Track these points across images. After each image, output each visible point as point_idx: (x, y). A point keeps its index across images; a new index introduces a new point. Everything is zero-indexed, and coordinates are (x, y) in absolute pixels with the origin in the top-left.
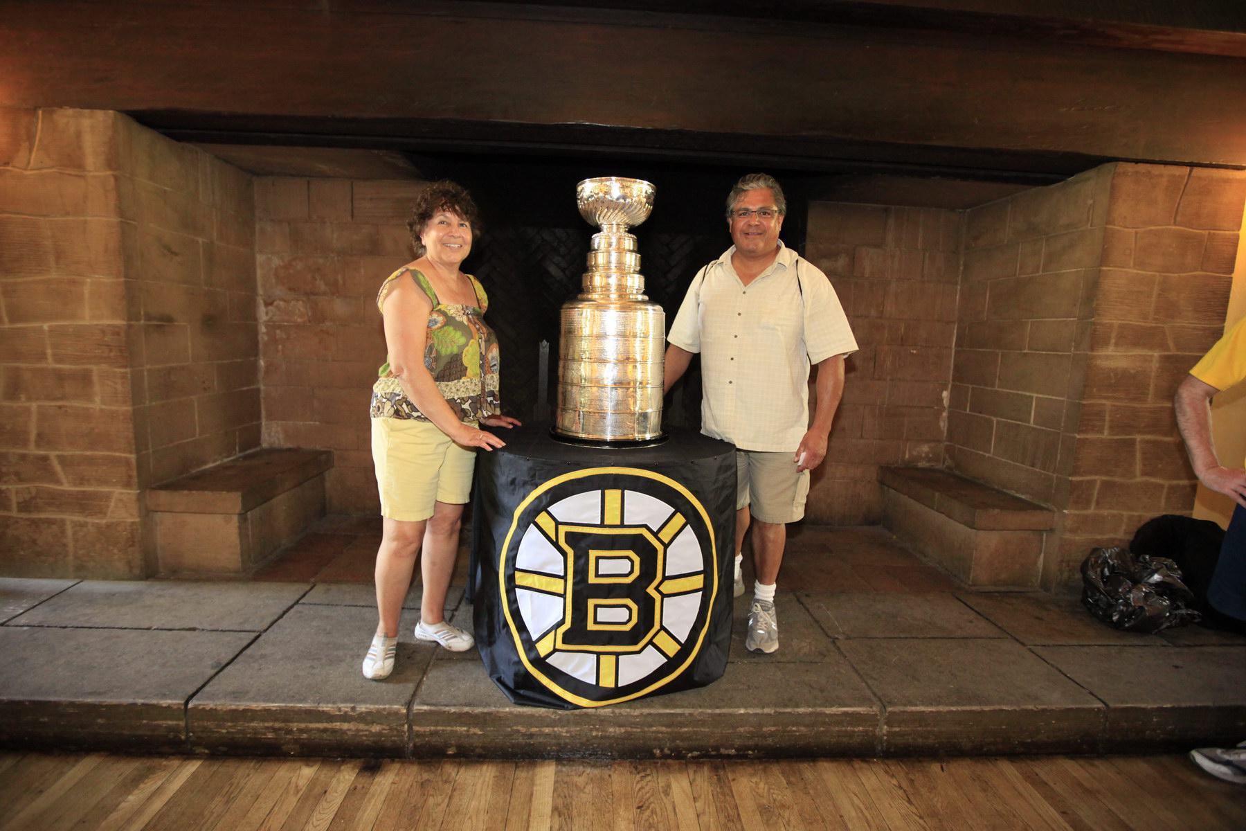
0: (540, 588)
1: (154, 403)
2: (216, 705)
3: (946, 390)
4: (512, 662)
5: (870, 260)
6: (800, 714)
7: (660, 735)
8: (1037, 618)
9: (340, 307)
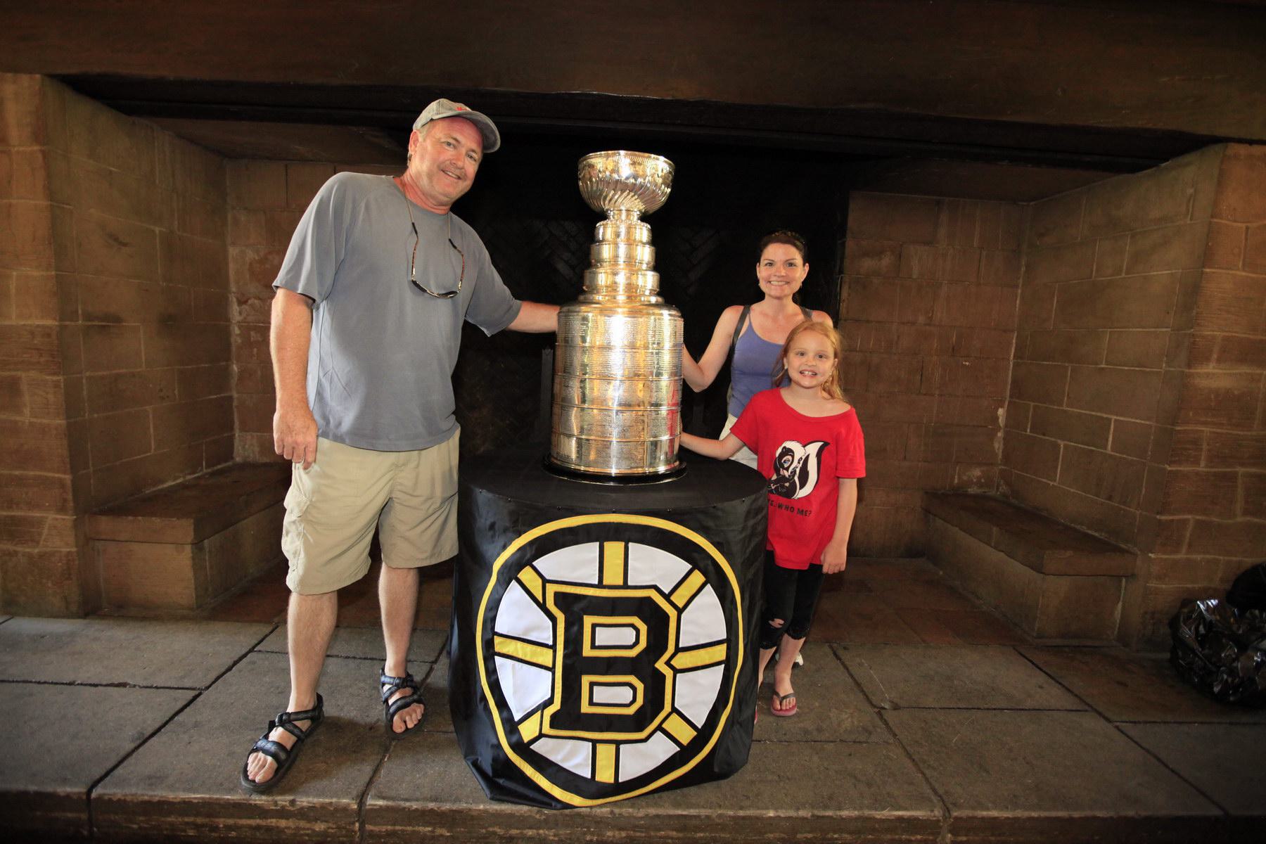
0: (523, 658)
1: (96, 415)
2: (126, 795)
3: (1001, 407)
4: (490, 745)
5: (919, 260)
6: (843, 819)
7: (670, 841)
8: (1120, 683)
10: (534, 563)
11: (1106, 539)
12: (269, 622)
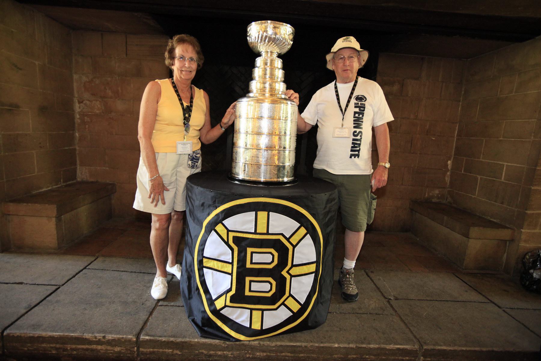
0: (217, 269)
2: (21, 334)
3: (450, 160)
4: (200, 312)
6: (372, 348)
7: (287, 358)
8: (505, 291)
9: (120, 105)
10: (223, 222)
11: (500, 223)
12: (94, 256)
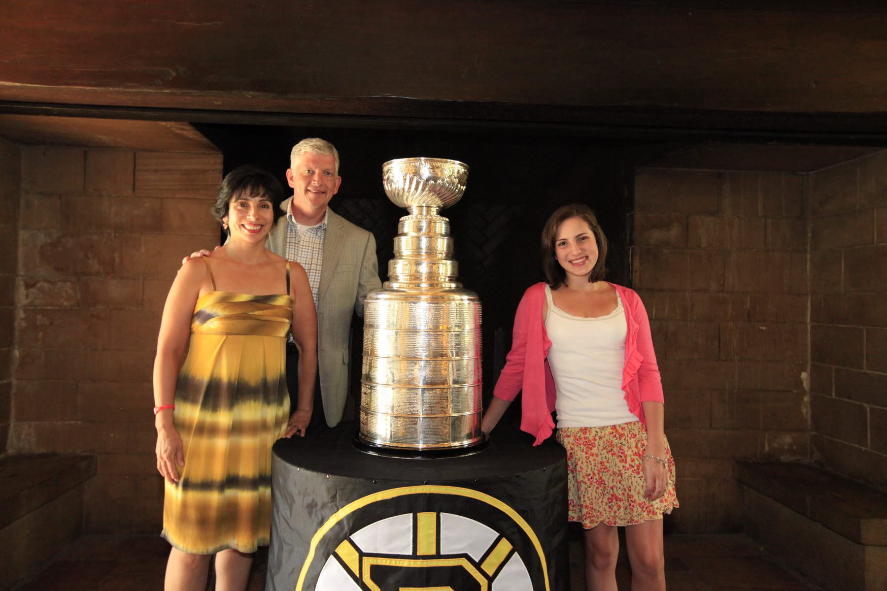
3: (805, 371)
9: (116, 289)
10: (351, 537)
